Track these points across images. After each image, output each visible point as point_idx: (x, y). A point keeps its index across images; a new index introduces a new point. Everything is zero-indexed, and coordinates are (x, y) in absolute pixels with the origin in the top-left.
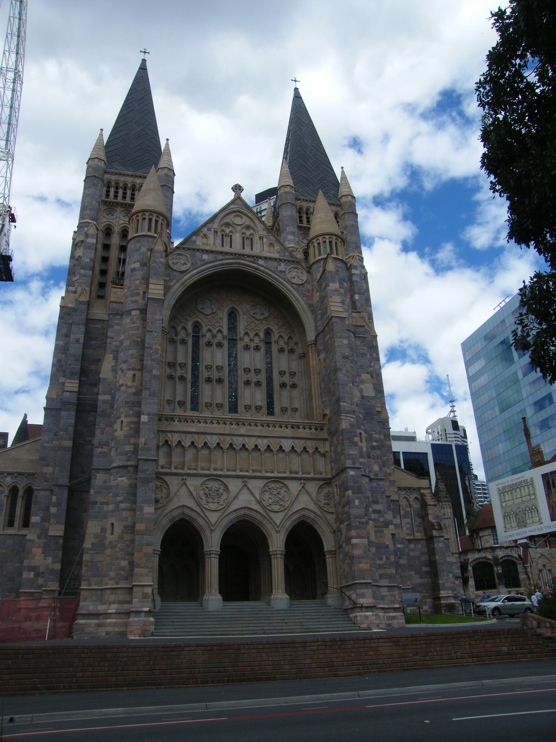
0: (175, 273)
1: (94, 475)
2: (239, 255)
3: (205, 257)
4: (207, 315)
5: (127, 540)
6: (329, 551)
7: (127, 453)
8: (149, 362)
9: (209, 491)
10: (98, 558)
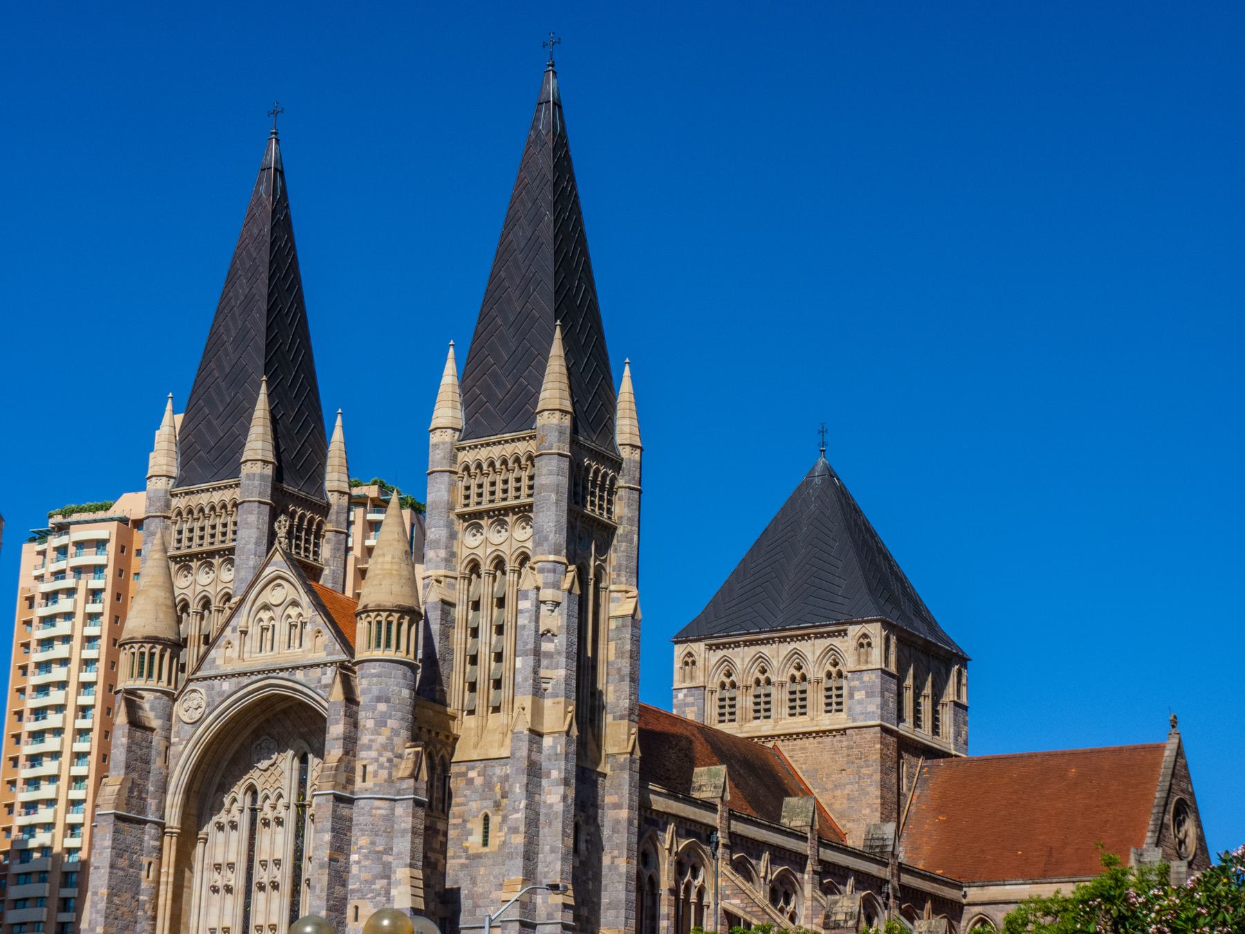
0: (187, 727)
2: (269, 671)
3: (226, 686)
4: (265, 770)
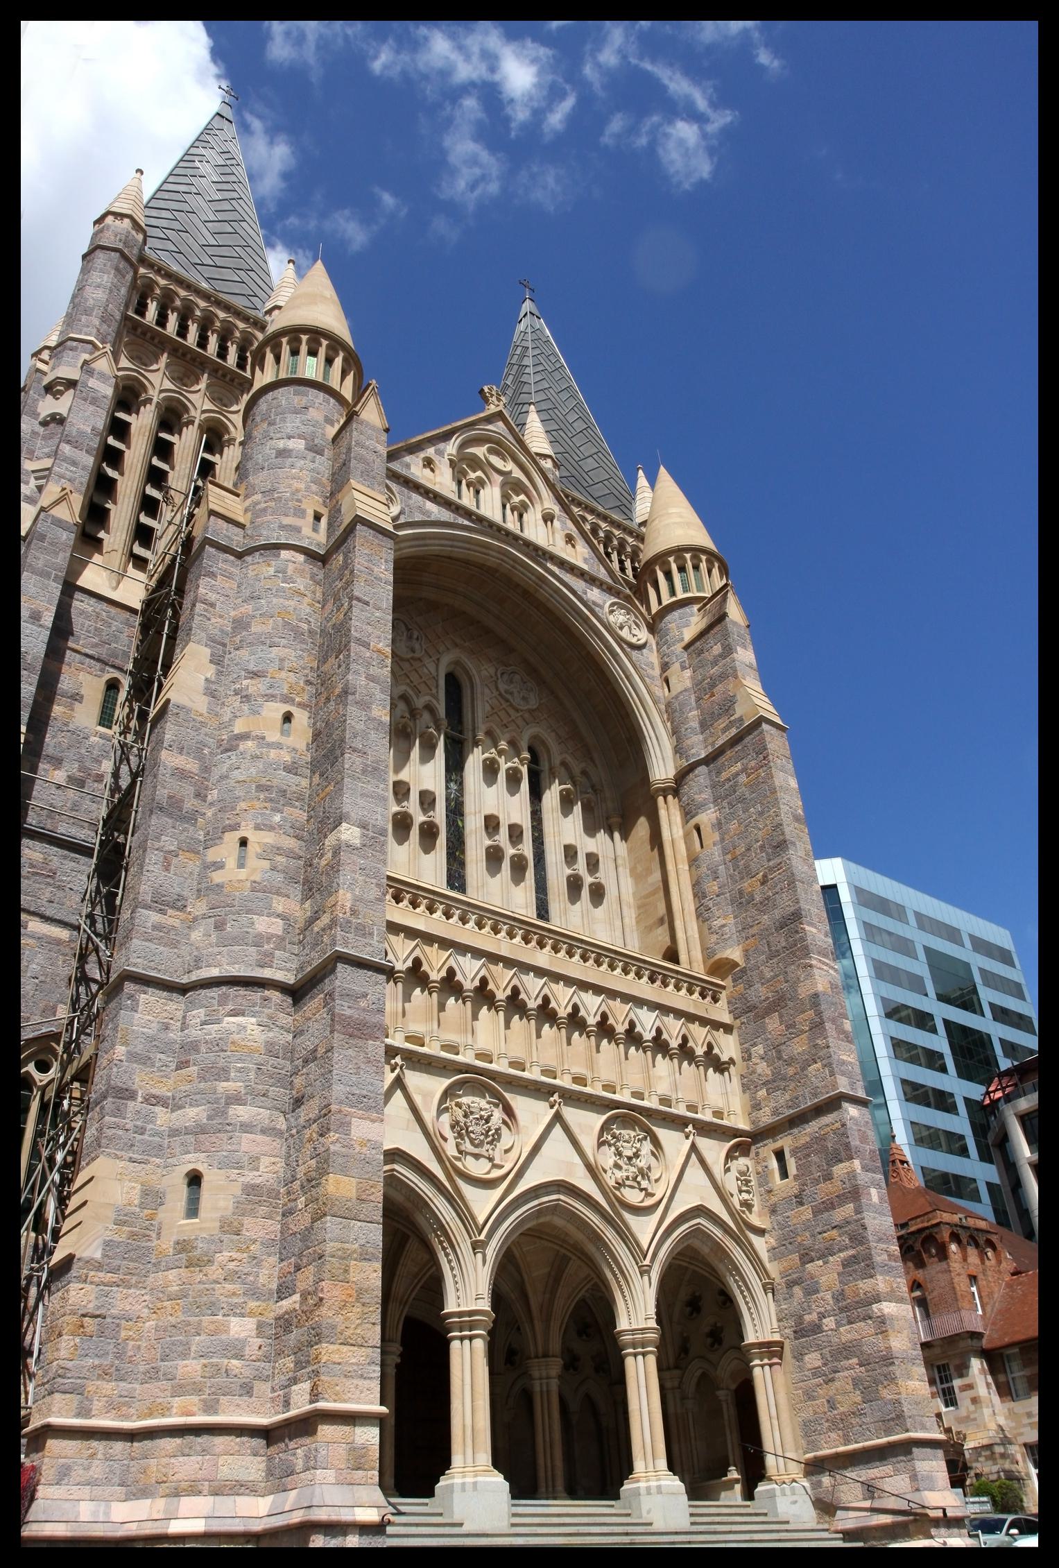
1: (131, 997)
5: (254, 1241)
6: (761, 1345)
7: (259, 940)
8: (362, 681)
9: (466, 1116)
10: (127, 1301)
